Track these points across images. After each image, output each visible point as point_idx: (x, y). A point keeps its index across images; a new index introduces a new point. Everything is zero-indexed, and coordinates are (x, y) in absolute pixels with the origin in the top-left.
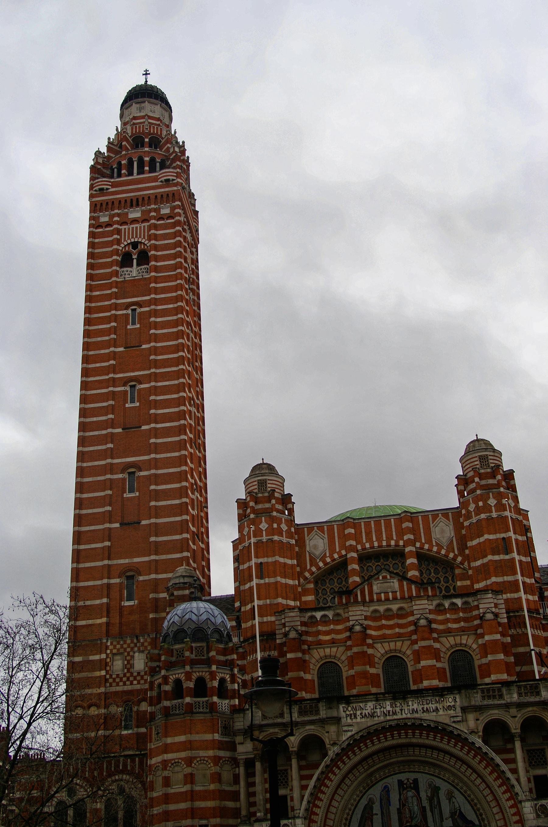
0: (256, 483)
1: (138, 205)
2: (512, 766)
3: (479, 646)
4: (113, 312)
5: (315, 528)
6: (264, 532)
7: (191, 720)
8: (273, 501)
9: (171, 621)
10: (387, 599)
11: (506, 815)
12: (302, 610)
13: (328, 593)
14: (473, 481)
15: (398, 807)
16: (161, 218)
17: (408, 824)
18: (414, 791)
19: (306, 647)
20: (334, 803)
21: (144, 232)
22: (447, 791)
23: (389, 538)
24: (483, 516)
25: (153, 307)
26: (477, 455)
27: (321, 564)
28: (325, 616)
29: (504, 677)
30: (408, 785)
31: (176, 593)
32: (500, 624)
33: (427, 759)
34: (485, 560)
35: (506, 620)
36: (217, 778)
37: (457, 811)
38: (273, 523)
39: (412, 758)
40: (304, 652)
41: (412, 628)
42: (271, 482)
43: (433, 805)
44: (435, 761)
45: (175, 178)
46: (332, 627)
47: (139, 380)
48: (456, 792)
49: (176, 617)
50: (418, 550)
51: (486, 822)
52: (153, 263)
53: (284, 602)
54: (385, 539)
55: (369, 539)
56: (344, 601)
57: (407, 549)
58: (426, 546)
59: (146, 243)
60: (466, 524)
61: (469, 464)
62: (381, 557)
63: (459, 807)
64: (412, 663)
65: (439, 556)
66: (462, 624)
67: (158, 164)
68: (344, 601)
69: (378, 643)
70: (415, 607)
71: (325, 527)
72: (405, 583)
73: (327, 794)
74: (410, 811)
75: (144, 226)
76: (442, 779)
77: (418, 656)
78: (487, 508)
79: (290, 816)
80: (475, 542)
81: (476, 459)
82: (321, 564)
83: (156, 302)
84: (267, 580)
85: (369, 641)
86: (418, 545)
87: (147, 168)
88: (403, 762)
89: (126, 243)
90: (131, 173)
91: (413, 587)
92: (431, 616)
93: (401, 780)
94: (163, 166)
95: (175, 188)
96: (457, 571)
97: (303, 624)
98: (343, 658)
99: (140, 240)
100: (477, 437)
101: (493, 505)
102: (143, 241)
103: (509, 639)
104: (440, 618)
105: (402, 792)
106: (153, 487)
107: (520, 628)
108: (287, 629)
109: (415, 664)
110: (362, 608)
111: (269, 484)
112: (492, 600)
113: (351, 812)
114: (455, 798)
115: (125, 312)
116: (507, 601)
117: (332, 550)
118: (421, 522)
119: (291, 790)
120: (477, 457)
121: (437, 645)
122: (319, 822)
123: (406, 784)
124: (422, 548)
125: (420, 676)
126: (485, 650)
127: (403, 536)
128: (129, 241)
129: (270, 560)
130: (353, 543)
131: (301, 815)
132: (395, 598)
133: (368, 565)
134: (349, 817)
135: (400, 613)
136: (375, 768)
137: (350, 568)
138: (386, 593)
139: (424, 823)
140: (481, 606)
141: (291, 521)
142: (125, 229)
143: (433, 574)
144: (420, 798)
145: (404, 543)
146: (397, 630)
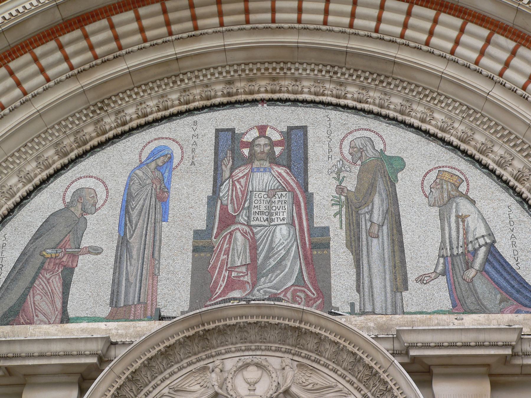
15: (202, 225)
17: (236, 294)
18: (282, 170)
22: (433, 176)
30: (258, 149)
33: (355, 44)
37: (475, 251)
39: (290, 39)
44: (391, 52)
63: (490, 234)
74: (254, 248)
76: (418, 130)
93: (232, 130)
105: (227, 174)
114: (473, 202)
123: (250, 145)
139: (313, 293)
144: (309, 199)
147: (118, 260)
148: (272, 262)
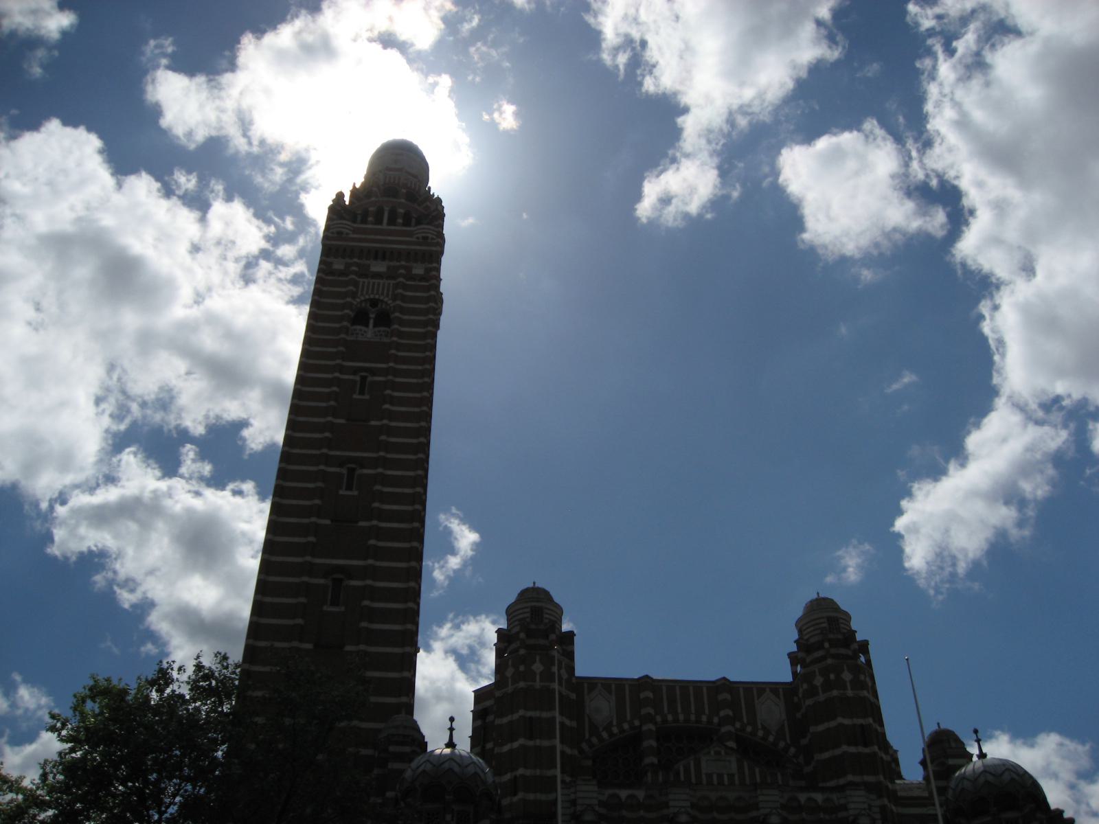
0: (528, 610)
1: (384, 258)
4: (337, 375)
6: (538, 677)
8: (553, 637)
9: (421, 769)
16: (413, 278)
21: (388, 290)
24: (835, 693)
25: (390, 377)
27: (605, 735)
28: (630, 797)
31: (392, 748)
34: (838, 752)
42: (549, 612)
45: (435, 237)
47: (362, 463)
52: (396, 326)
54: (693, 712)
56: (660, 779)
57: (726, 729)
58: (749, 729)
59: (390, 302)
60: (809, 702)
67: (414, 220)
68: (660, 779)
71: (613, 686)
72: (746, 764)
75: (389, 284)
80: (821, 728)
81: (822, 620)
82: (605, 735)
83: (396, 373)
84: (538, 742)
86: (738, 725)
87: (400, 221)
89: (362, 298)
90: (379, 221)
91: (757, 770)
94: (418, 223)
95: (434, 249)
99: (382, 298)
100: (818, 596)
102: (386, 299)
106: (366, 603)
108: (579, 808)
111: (547, 613)
115: (351, 377)
128: (367, 297)
129: (545, 715)
130: (652, 711)
137: (646, 744)
138: (720, 776)
140: (852, 806)
141: (571, 669)
142: (364, 282)
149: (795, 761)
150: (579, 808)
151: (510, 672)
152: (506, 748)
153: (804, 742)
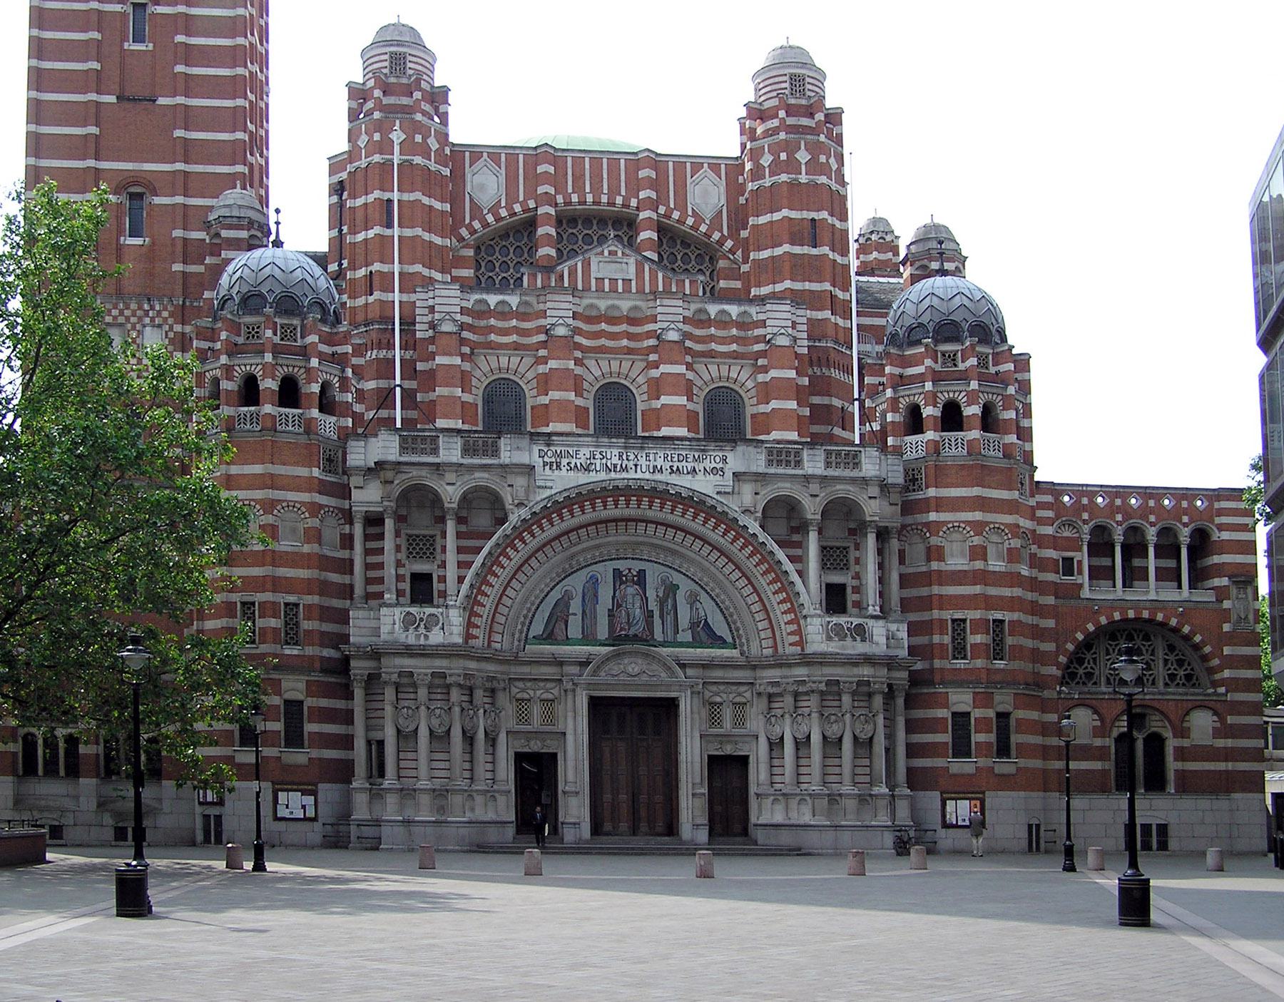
2: (799, 566)
3: (758, 385)
5: (485, 154)
7: (272, 441)
10: (614, 290)
11: (778, 634)
12: (466, 286)
13: (497, 270)
14: (776, 116)
15: (611, 608)
17: (623, 633)
18: (637, 587)
19: (466, 350)
20: (510, 592)
23: (614, 191)
24: (784, 177)
26: (786, 71)
28: (503, 302)
29: (793, 436)
32: (797, 355)
33: (665, 544)
34: (778, 251)
35: (805, 351)
36: (314, 536)
38: (416, 131)
39: (641, 539)
40: (463, 356)
41: (652, 342)
43: (665, 610)
44: (677, 548)
46: (514, 322)
48: (703, 597)
49: (246, 270)
50: (662, 219)
51: (744, 640)
53: (426, 272)
54: (605, 191)
55: (579, 187)
56: (539, 284)
58: (676, 215)
60: (750, 186)
61: (770, 85)
62: (595, 222)
64: (645, 397)
65: (695, 234)
66: (734, 347)
68: (539, 284)
69: (591, 358)
70: (659, 309)
71: (503, 156)
73: (501, 578)
77: (656, 388)
78: (793, 166)
79: (435, 602)
80: (763, 220)
85: (578, 354)
86: (662, 210)
88: (625, 543)
91: (660, 275)
92: (687, 328)
96: (722, 264)
97: (463, 311)
98: (530, 375)
101: (803, 162)
103: (806, 381)
104: (698, 332)
107: (820, 366)
108: (437, 316)
109: (649, 400)
110: (570, 298)
112: (788, 315)
113: (533, 608)
116: (811, 322)
117: (512, 197)
118: (671, 173)
119: (443, 565)
120: (786, 75)
121: (690, 375)
122: (485, 617)
124: (668, 216)
125: (655, 419)
126: (766, 391)
127: (639, 191)
131: (458, 603)
132: (627, 290)
133: (571, 231)
134: (530, 615)
135: (632, 315)
136: (580, 547)
137: (541, 231)
138: (613, 281)
141: (443, 137)
143: (679, 262)
144: (647, 599)
145: (638, 203)
146: (625, 342)
147: (583, 619)
148: (635, 622)
149: (732, 257)
150: (437, 316)
151: (362, 143)
152: (360, 237)
153: (744, 234)
